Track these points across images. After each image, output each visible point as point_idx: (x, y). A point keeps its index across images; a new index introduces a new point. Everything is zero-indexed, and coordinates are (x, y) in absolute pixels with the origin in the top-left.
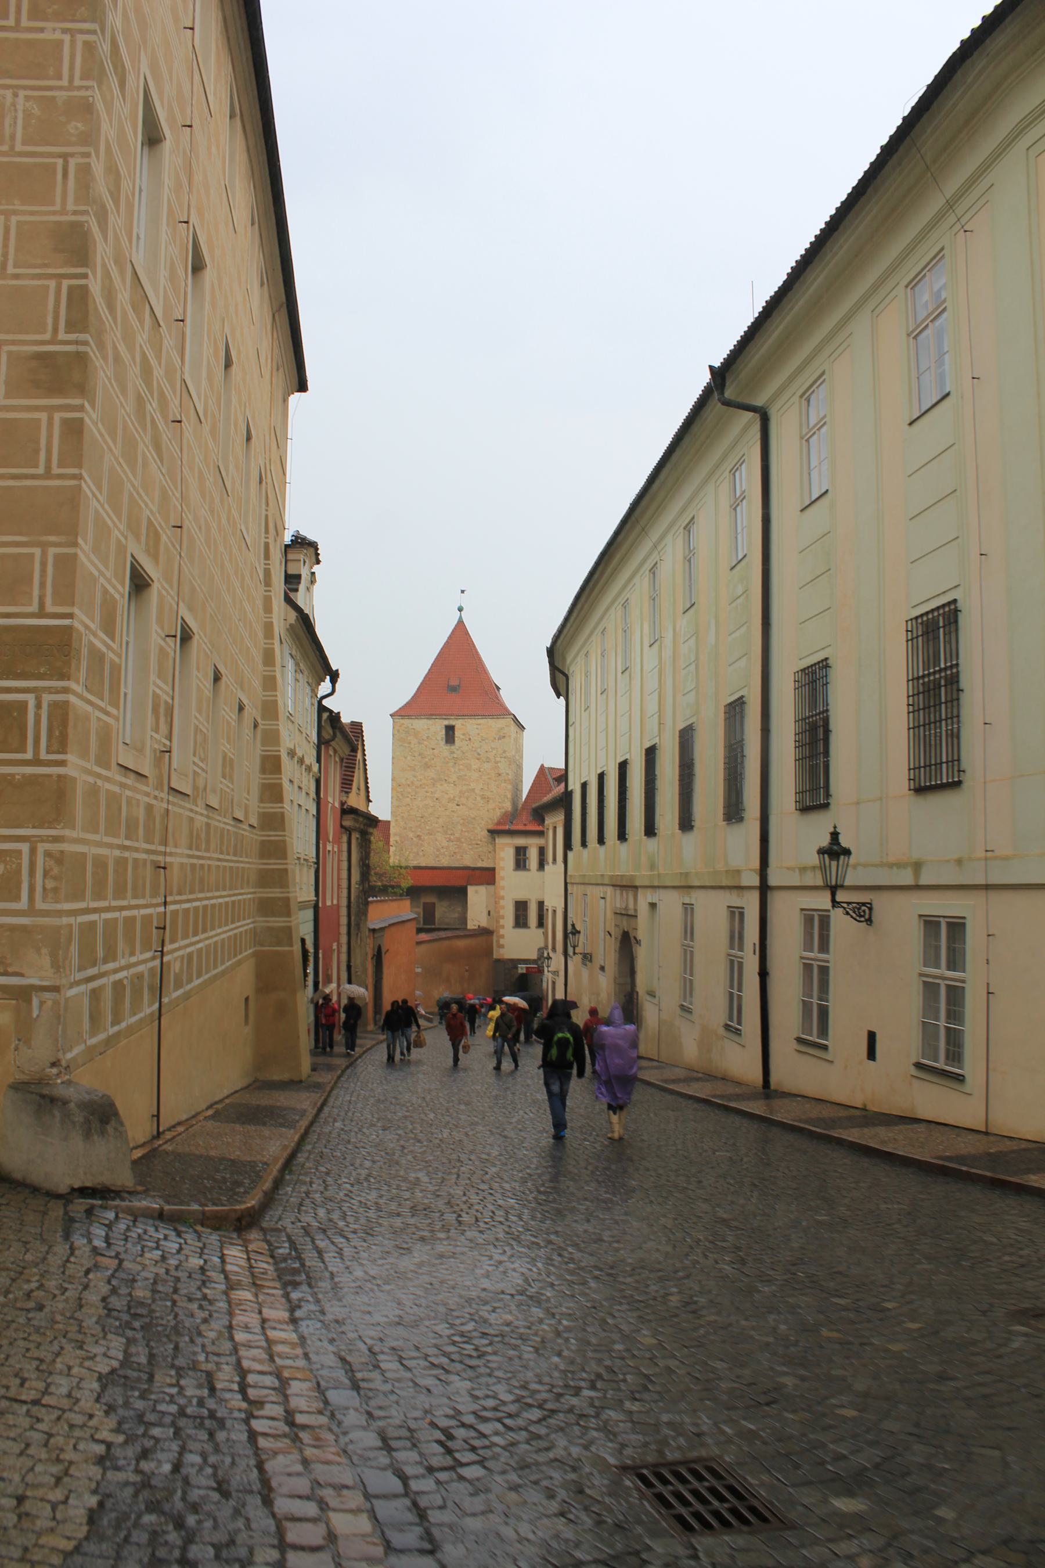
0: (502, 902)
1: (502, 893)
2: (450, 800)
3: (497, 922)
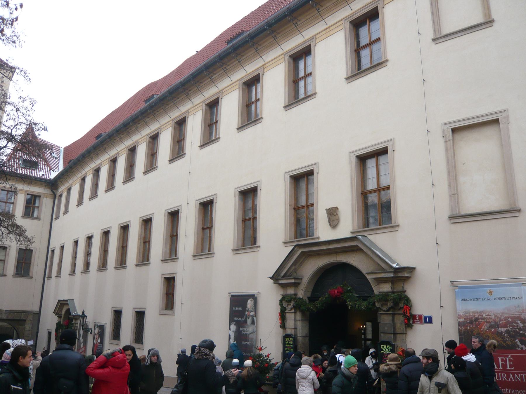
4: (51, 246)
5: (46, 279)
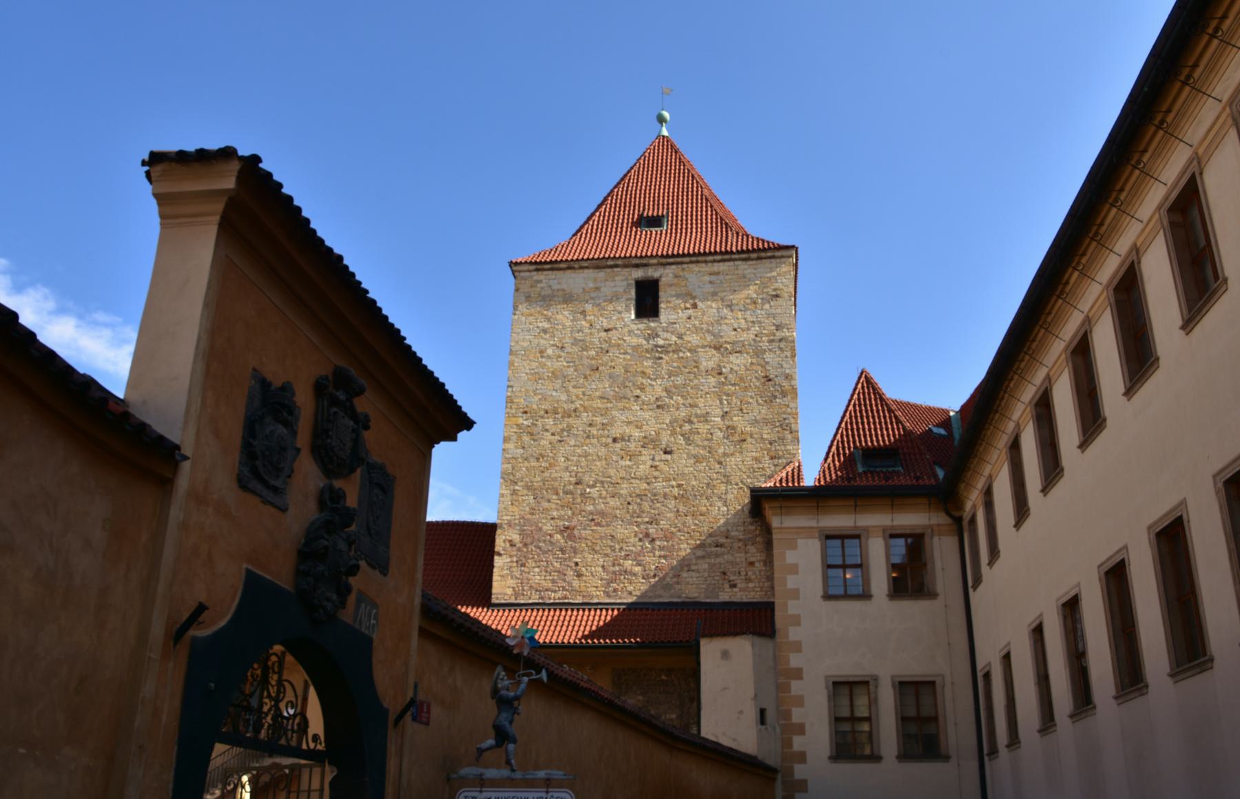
0: (796, 687)
1: (795, 661)
2: (648, 442)
3: (788, 743)
4: (980, 665)
5: (986, 758)
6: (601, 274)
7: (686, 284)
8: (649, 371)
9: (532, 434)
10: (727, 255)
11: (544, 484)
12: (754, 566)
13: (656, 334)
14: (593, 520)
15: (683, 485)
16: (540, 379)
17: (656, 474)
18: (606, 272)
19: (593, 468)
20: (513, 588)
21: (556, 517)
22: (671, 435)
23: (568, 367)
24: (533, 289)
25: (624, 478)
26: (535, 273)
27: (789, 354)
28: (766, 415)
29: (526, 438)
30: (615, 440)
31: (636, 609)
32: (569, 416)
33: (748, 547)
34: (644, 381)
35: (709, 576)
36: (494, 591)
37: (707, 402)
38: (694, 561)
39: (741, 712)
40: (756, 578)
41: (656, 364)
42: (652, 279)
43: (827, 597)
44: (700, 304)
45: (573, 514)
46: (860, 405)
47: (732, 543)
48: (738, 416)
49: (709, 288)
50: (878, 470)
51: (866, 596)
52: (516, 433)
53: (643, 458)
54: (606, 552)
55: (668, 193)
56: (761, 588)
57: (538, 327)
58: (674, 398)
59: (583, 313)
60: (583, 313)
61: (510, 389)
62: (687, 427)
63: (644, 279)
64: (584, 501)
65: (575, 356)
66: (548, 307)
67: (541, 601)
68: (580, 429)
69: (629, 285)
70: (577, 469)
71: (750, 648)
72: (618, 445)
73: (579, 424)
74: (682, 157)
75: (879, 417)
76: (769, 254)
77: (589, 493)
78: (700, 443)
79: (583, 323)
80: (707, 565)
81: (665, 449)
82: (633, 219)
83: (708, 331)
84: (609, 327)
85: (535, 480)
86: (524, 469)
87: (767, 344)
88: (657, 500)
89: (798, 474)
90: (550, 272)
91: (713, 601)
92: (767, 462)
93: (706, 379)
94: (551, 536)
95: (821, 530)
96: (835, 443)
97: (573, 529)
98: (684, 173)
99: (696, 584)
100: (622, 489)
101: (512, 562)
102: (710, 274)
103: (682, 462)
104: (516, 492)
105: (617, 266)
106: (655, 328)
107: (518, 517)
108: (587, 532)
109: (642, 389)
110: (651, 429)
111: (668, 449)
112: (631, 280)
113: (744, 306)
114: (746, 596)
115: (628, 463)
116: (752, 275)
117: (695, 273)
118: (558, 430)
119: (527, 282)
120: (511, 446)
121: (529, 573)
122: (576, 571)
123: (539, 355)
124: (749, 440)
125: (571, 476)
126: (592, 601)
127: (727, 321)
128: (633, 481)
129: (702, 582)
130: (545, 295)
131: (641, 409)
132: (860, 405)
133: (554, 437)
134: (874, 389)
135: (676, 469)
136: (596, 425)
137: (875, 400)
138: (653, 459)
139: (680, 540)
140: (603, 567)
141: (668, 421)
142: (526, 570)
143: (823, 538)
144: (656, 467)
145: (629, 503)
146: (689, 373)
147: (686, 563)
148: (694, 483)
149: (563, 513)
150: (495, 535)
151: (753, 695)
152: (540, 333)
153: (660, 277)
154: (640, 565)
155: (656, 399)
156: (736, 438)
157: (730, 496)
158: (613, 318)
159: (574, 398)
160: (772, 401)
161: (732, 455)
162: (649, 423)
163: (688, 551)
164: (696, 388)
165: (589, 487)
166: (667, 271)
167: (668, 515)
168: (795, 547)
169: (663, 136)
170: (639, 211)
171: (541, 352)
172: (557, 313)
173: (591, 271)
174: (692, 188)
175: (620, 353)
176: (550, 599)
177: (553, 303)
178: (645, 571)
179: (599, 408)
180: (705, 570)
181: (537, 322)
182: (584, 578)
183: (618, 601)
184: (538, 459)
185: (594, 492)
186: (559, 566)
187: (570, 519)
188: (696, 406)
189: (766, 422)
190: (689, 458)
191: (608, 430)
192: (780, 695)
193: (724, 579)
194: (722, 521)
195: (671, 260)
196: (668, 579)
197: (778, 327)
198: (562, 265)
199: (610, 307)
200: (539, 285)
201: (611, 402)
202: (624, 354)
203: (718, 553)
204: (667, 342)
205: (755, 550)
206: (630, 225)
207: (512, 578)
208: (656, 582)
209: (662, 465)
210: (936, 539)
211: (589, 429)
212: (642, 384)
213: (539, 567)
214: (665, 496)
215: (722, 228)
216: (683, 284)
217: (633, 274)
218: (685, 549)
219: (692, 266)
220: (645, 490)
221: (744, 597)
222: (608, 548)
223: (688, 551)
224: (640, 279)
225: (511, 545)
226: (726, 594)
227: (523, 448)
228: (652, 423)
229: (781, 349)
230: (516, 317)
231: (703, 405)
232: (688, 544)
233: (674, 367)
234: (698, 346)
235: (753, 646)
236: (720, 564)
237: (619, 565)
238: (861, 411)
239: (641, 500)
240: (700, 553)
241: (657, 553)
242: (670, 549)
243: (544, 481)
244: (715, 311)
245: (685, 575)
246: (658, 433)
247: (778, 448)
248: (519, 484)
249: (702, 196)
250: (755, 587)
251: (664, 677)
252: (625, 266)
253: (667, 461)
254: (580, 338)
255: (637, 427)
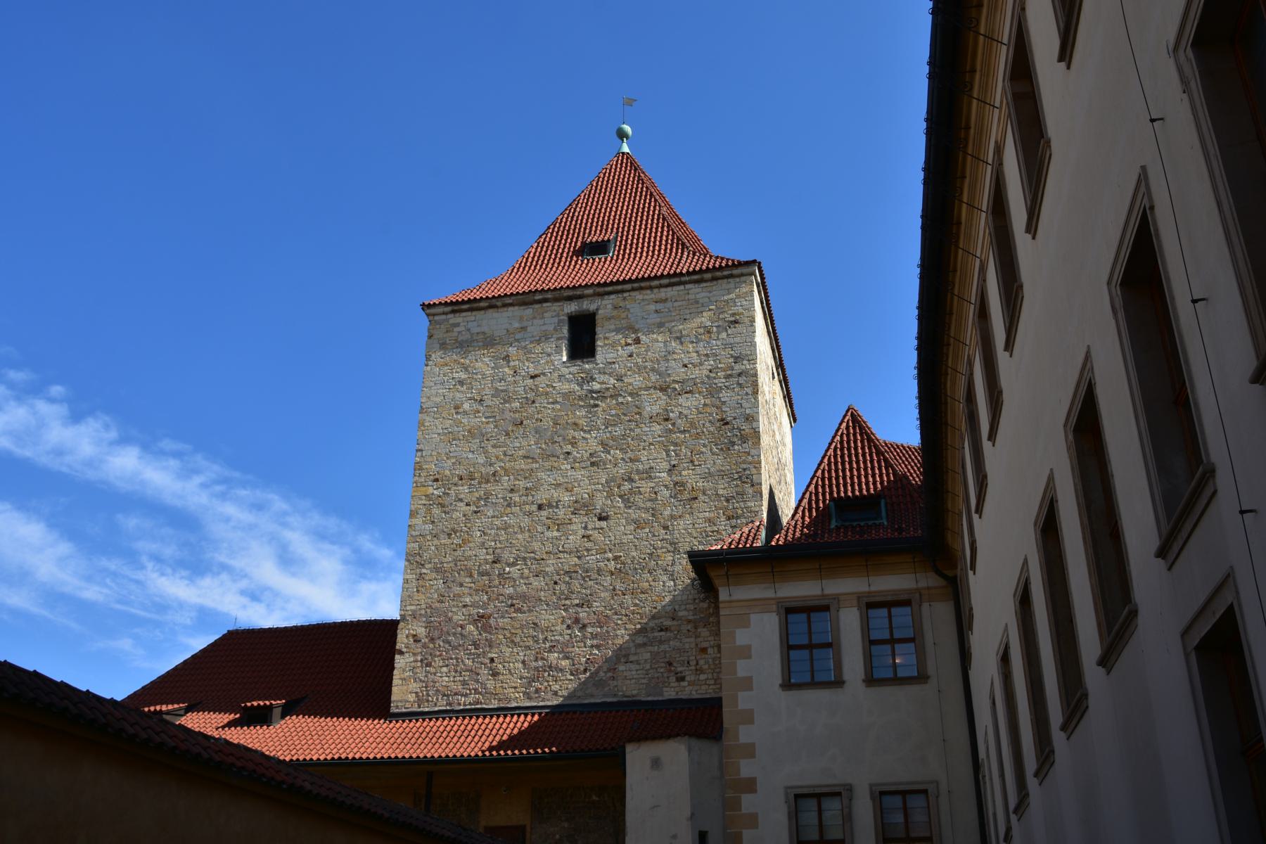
0: (748, 803)
1: (746, 769)
2: (581, 507)
6: (529, 311)
7: (627, 316)
8: (582, 422)
9: (443, 506)
10: (675, 279)
11: (456, 565)
12: (707, 654)
13: (591, 377)
14: (512, 605)
15: (621, 556)
16: (454, 439)
17: (589, 545)
18: (533, 309)
19: (514, 542)
20: (416, 693)
21: (469, 603)
22: (607, 497)
23: (487, 423)
24: (449, 334)
25: (550, 553)
26: (452, 316)
27: (749, 391)
28: (722, 466)
29: (436, 511)
30: (540, 507)
31: (561, 713)
32: (488, 481)
33: (699, 630)
34: (576, 434)
35: (652, 668)
36: (393, 698)
37: (650, 454)
38: (633, 650)
39: (674, 837)
40: (709, 668)
41: (590, 413)
42: (588, 313)
43: (787, 685)
44: (643, 338)
45: (489, 599)
46: (842, 450)
47: (680, 625)
48: (689, 469)
49: (655, 319)
50: (855, 524)
51: (838, 683)
52: (425, 505)
53: (574, 527)
54: (527, 644)
55: (620, 215)
56: (715, 680)
57: (453, 378)
58: (612, 452)
59: (507, 358)
60: (507, 358)
61: (419, 454)
62: (627, 486)
63: (578, 314)
64: (502, 583)
65: (496, 410)
66: (465, 355)
67: (448, 708)
68: (499, 496)
69: (560, 321)
70: (496, 544)
71: (687, 754)
72: (544, 513)
73: (498, 490)
74: (642, 175)
75: (865, 462)
76: (726, 273)
77: (509, 573)
78: (643, 505)
79: (506, 370)
80: (649, 654)
81: (600, 514)
82: (574, 247)
83: (653, 370)
84: (536, 372)
85: (446, 560)
86: (433, 548)
87: (724, 381)
88: (588, 576)
89: (755, 535)
90: (469, 313)
91: (655, 699)
92: (723, 523)
93: (650, 427)
94: (462, 627)
95: (779, 601)
96: (807, 495)
97: (489, 618)
98: (641, 193)
99: (635, 679)
100: (548, 566)
101: (416, 661)
102: (656, 302)
103: (620, 529)
104: (423, 575)
105: (546, 300)
106: (590, 370)
107: (424, 606)
108: (505, 620)
109: (574, 444)
110: (583, 492)
111: (604, 514)
112: (563, 315)
113: (696, 337)
114: (697, 691)
115: (556, 534)
116: (707, 300)
117: (638, 302)
118: (474, 499)
119: (442, 326)
120: (418, 521)
121: (435, 674)
122: (491, 669)
123: (454, 411)
124: (702, 497)
125: (487, 554)
126: (509, 706)
127: (675, 356)
128: (561, 555)
129: (642, 676)
130: (462, 340)
131: (572, 468)
132: (842, 450)
133: (469, 507)
134: (861, 428)
135: (613, 538)
136: (519, 491)
137: (862, 442)
138: (586, 528)
139: (617, 624)
140: (523, 662)
141: (603, 481)
142: (432, 670)
143: (783, 611)
144: (588, 537)
145: (556, 583)
146: (630, 421)
147: (624, 653)
148: (634, 554)
149: (477, 598)
150: (397, 629)
151: (689, 813)
152: (455, 385)
153: (597, 309)
154: (568, 658)
155: (591, 454)
156: (686, 496)
157: (678, 568)
158: (542, 362)
159: (494, 459)
160: (729, 449)
161: (680, 517)
162: (582, 484)
163: (627, 638)
164: (638, 438)
165: (509, 565)
166: (604, 302)
167: (602, 595)
168: (747, 625)
169: (623, 153)
170: (583, 238)
171: (457, 407)
172: (476, 360)
173: (516, 308)
174: (649, 208)
175: (548, 403)
176: (460, 704)
177: (471, 349)
178: (574, 665)
179: (522, 470)
180: (646, 660)
181: (452, 373)
182: (501, 677)
183: (541, 704)
184: (449, 535)
185: (514, 571)
186: (471, 664)
187: (485, 606)
188: (638, 460)
189: (722, 474)
190: (628, 523)
191: (533, 496)
192: (727, 813)
193: (670, 671)
194: (667, 599)
195: (610, 289)
196: (602, 674)
197: (737, 359)
198: (483, 304)
199: (538, 349)
200: (456, 329)
201: (537, 462)
202: (553, 403)
203: (663, 639)
204: (604, 386)
205: (707, 633)
206: (570, 254)
207: (415, 681)
208: (590, 677)
209: (595, 534)
210: (925, 606)
211: (510, 495)
212: (574, 438)
213: (447, 666)
214: (599, 571)
215: (677, 249)
216: (624, 315)
217: (565, 307)
218: (622, 636)
219: (633, 294)
220: (576, 565)
221: (694, 693)
222: (529, 639)
223: (627, 638)
224: (574, 314)
225: (415, 641)
226: (672, 689)
227: (433, 522)
228: (584, 483)
229: (740, 385)
230: (429, 368)
231: (646, 458)
232: (626, 629)
233: (612, 416)
234: (640, 389)
235: (690, 751)
236: (665, 652)
237: (543, 659)
238: (842, 456)
239: (571, 578)
240: (640, 640)
241: (589, 642)
242: (605, 637)
243: (455, 561)
244: (662, 345)
245: (622, 668)
246: (591, 496)
247: (736, 505)
248: (427, 566)
249: (659, 215)
250: (708, 679)
251: (594, 798)
252: (556, 300)
253: (602, 529)
254: (502, 388)
255: (567, 490)
